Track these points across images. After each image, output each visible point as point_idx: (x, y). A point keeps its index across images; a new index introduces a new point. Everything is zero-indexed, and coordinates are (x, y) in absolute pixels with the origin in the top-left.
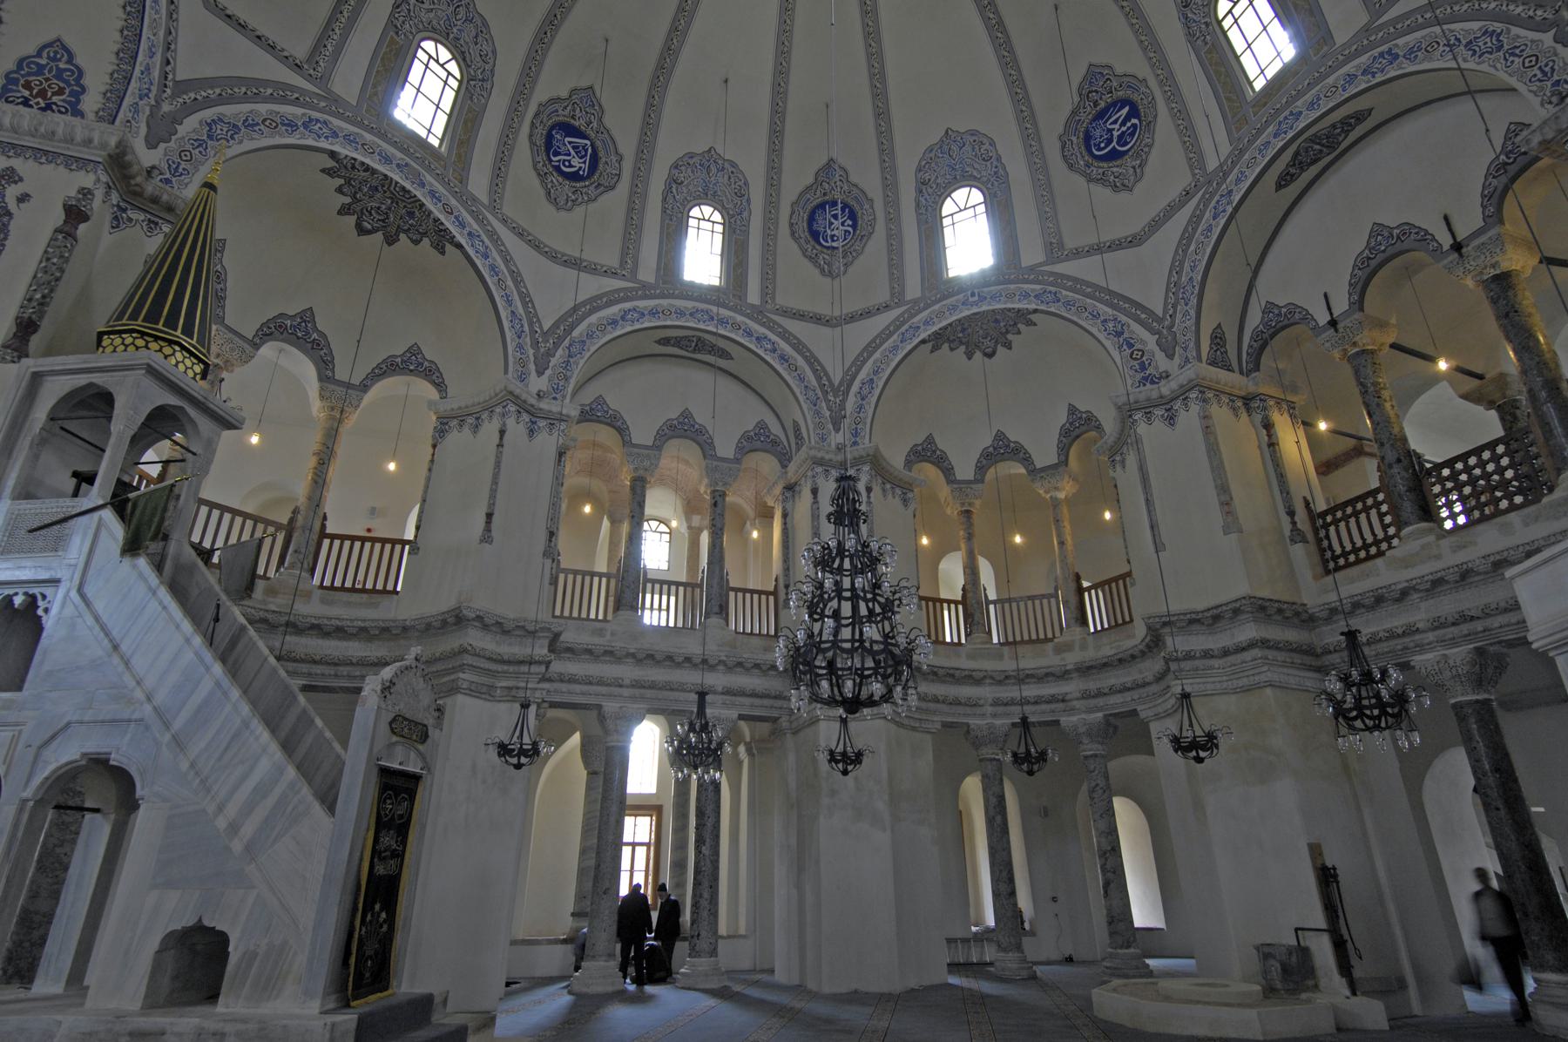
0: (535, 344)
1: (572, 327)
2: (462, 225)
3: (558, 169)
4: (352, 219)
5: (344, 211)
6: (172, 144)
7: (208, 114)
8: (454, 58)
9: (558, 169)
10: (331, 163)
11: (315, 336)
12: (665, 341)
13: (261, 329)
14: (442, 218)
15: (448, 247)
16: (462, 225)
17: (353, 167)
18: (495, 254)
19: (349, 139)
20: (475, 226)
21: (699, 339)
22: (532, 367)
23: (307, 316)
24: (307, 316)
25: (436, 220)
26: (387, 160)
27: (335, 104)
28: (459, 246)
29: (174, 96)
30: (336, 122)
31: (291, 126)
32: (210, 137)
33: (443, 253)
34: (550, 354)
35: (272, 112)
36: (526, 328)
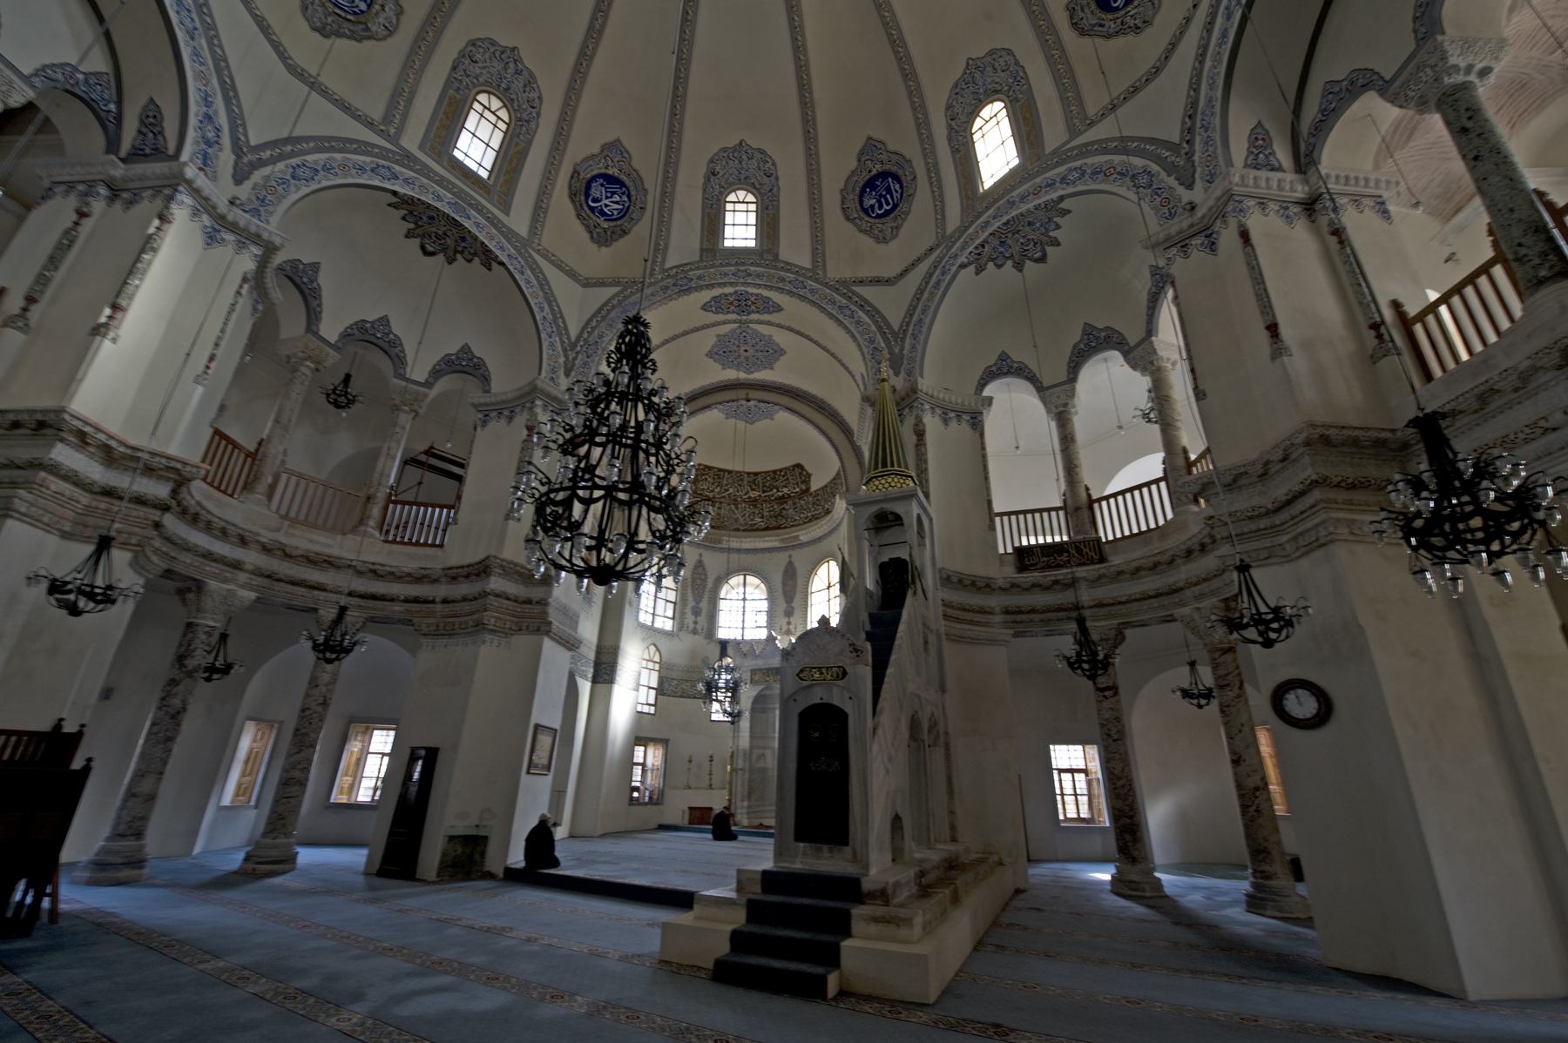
0: (1170, 169)
1: (1194, 104)
5: (1019, 266)
10: (972, 268)
14: (1037, 202)
15: (1063, 205)
16: (1051, 185)
18: (1089, 161)
19: (963, 248)
20: (1062, 169)
22: (1181, 190)
23: (1089, 331)
24: (1089, 331)
26: (987, 223)
28: (1062, 198)
31: (938, 282)
34: (1189, 155)
36: (1155, 168)
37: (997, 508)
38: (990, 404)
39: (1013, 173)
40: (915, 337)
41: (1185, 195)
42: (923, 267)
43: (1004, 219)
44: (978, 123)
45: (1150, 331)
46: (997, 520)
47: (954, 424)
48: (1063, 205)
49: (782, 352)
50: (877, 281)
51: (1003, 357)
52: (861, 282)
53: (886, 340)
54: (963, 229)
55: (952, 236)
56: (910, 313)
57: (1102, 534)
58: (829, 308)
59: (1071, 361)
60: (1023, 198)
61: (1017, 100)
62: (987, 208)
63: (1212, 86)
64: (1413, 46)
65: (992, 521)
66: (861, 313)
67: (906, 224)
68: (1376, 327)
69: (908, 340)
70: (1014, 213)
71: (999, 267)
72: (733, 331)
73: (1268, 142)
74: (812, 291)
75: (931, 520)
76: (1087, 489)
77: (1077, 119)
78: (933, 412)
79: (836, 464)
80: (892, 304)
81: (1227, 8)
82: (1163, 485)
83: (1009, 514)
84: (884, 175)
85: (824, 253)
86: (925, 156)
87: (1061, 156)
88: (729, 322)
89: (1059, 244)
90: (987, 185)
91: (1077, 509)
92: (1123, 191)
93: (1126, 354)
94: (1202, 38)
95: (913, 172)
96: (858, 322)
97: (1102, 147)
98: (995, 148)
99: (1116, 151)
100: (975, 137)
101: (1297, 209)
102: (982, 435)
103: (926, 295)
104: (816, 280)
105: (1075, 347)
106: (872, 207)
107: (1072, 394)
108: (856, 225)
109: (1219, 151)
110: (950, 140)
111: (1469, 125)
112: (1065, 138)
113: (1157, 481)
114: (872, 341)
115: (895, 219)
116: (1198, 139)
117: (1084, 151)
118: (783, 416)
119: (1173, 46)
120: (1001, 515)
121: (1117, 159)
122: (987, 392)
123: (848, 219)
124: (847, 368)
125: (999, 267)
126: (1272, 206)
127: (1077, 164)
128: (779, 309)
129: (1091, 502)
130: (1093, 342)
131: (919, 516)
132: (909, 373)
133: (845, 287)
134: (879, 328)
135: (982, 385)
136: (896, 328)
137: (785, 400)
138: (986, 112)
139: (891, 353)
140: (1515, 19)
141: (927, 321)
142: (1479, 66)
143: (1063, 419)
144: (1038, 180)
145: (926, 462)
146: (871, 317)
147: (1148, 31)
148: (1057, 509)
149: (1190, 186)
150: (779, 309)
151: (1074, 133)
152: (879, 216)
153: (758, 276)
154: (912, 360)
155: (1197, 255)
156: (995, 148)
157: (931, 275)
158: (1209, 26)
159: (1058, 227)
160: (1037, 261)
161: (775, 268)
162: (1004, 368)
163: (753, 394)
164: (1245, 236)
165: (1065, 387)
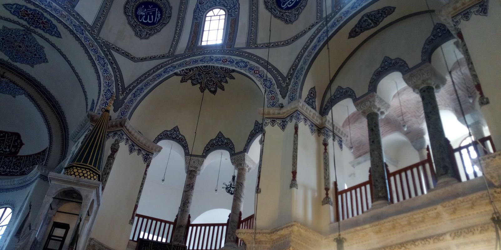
0: (279, 86)
1: (296, 66)
2: (232, 62)
3: (288, 9)
4: (207, 91)
5: (202, 90)
6: (123, 107)
7: (134, 91)
8: (221, 9)
9: (288, 9)
10: (180, 78)
11: (226, 141)
12: (353, 34)
13: (205, 149)
14: (222, 66)
15: (234, 74)
16: (232, 62)
17: (187, 73)
18: (251, 62)
19: (180, 65)
20: (239, 58)
21: (368, 15)
22: (280, 96)
25: (221, 68)
26: (196, 61)
27: (176, 58)
28: (233, 71)
29: (122, 93)
30: (175, 63)
31: (160, 75)
32: (134, 97)
33: (234, 78)
34: (288, 85)
35: (153, 76)
36: (274, 82)
37: (138, 212)
38: (159, 151)
39: (216, 46)
40: (135, 95)
41: (281, 100)
42: (155, 63)
43: (205, 64)
44: (210, 13)
45: (246, 150)
46: (136, 218)
47: (135, 153)
48: (234, 74)
49: (45, 60)
50: (127, 55)
51: (176, 129)
52: (118, 50)
53: (117, 89)
54: (183, 56)
55: (177, 56)
56: (138, 81)
57: (187, 245)
58: (92, 53)
59: (207, 146)
60: (217, 60)
61: (231, 16)
62: (199, 54)
63: (305, 63)
64: (366, 91)
65: (133, 218)
66: (109, 66)
67: (155, 36)
68: (327, 189)
69: (130, 96)
70: (211, 64)
71: (193, 84)
72: (18, 30)
73: (314, 97)
74: (86, 38)
75: (99, 205)
76: (189, 217)
77: (252, 41)
78: (127, 142)
79: (46, 145)
80: (130, 71)
81: (319, 38)
82: (225, 227)
83: (144, 217)
84: (155, 5)
85: (103, 23)
86: (180, 11)
87: (240, 52)
88: (19, 24)
89: (224, 90)
90: (204, 44)
91: (181, 226)
92: (259, 83)
93: (232, 155)
94: (307, 42)
95: (170, 14)
96: (106, 71)
97: (258, 59)
98: (214, 29)
99: (262, 65)
100: (207, 19)
101: (316, 128)
102: (148, 166)
103: (151, 77)
104: (91, 34)
105: (211, 140)
106: (141, 16)
107: (201, 163)
108: (128, 19)
109: (299, 90)
110: (195, 12)
111: (374, 129)
112: (244, 46)
113: (223, 225)
114: (109, 85)
115: (151, 30)
116: (293, 80)
117: (251, 56)
118: (22, 99)
119: (296, 38)
120: (139, 216)
121: (261, 68)
122: (160, 144)
123: (125, 13)
124: (85, 92)
125: (193, 84)
126: (308, 123)
127: (245, 60)
128: (59, 36)
129: (189, 224)
130: (220, 143)
131: (93, 200)
132: (123, 114)
133: (108, 48)
134: (116, 81)
135: (159, 139)
136: (126, 84)
137: (31, 90)
138: (216, 11)
139: (117, 97)
140: (394, 100)
141: (146, 91)
142: (382, 110)
143: (192, 173)
144: (227, 56)
145: (110, 168)
146: (115, 72)
147: (290, 25)
148: (170, 223)
149: (284, 97)
150: (59, 36)
151: (248, 45)
152: (142, 22)
153: (56, 10)
154: (127, 107)
155: (277, 128)
156: (214, 29)
157: (158, 69)
158: (311, 40)
159: (226, 82)
160: (211, 91)
161: (69, 12)
162: (174, 135)
163: (9, 75)
164: (296, 129)
165: (200, 159)
